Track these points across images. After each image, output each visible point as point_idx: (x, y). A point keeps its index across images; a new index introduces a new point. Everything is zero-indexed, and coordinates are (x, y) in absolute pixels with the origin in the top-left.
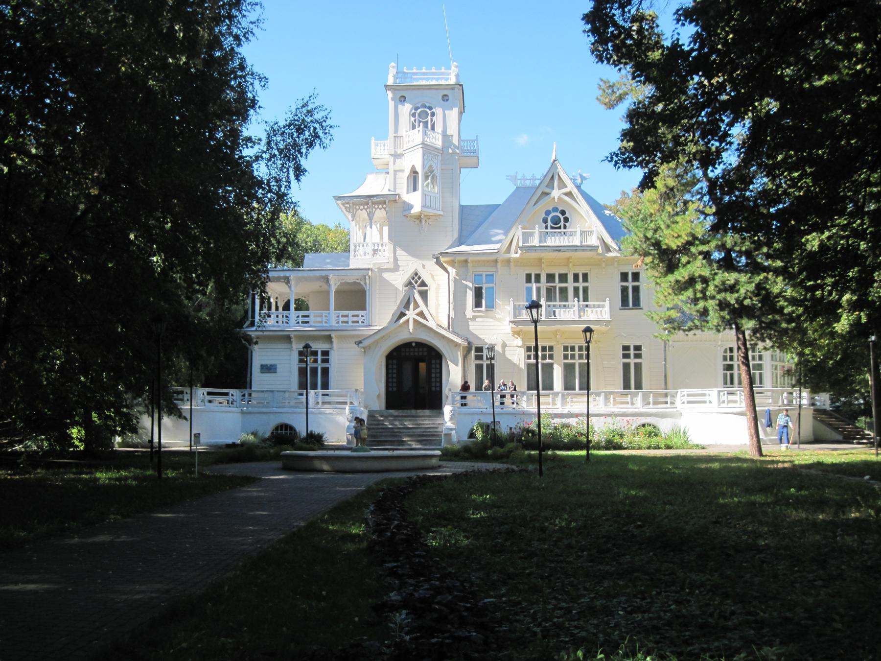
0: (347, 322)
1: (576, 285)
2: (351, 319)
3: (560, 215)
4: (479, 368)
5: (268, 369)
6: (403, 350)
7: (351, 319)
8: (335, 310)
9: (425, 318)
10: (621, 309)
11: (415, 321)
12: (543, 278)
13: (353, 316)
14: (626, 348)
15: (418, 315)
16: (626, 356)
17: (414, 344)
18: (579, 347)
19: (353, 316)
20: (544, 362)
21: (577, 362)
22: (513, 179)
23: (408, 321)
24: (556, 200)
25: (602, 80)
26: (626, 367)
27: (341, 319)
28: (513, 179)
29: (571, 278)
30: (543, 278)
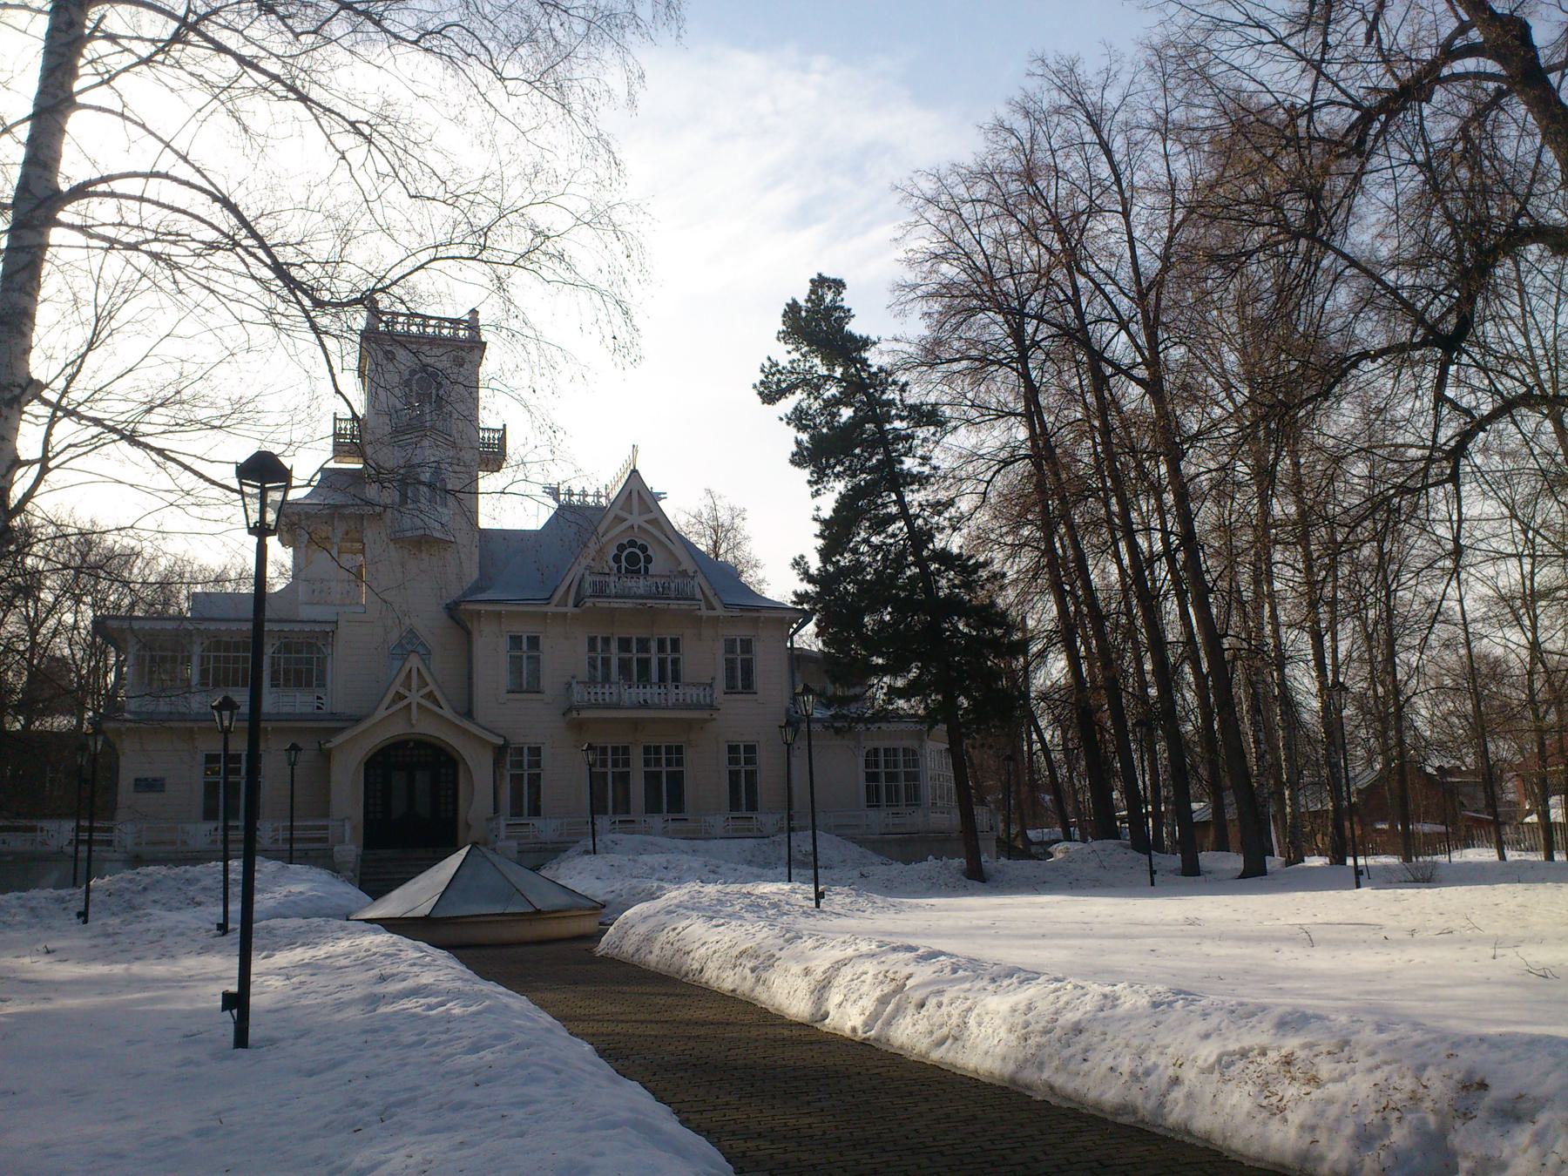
1: (662, 655)
4: (517, 779)
12: (614, 645)
14: (733, 749)
20: (670, 769)
26: (734, 775)
30: (614, 645)
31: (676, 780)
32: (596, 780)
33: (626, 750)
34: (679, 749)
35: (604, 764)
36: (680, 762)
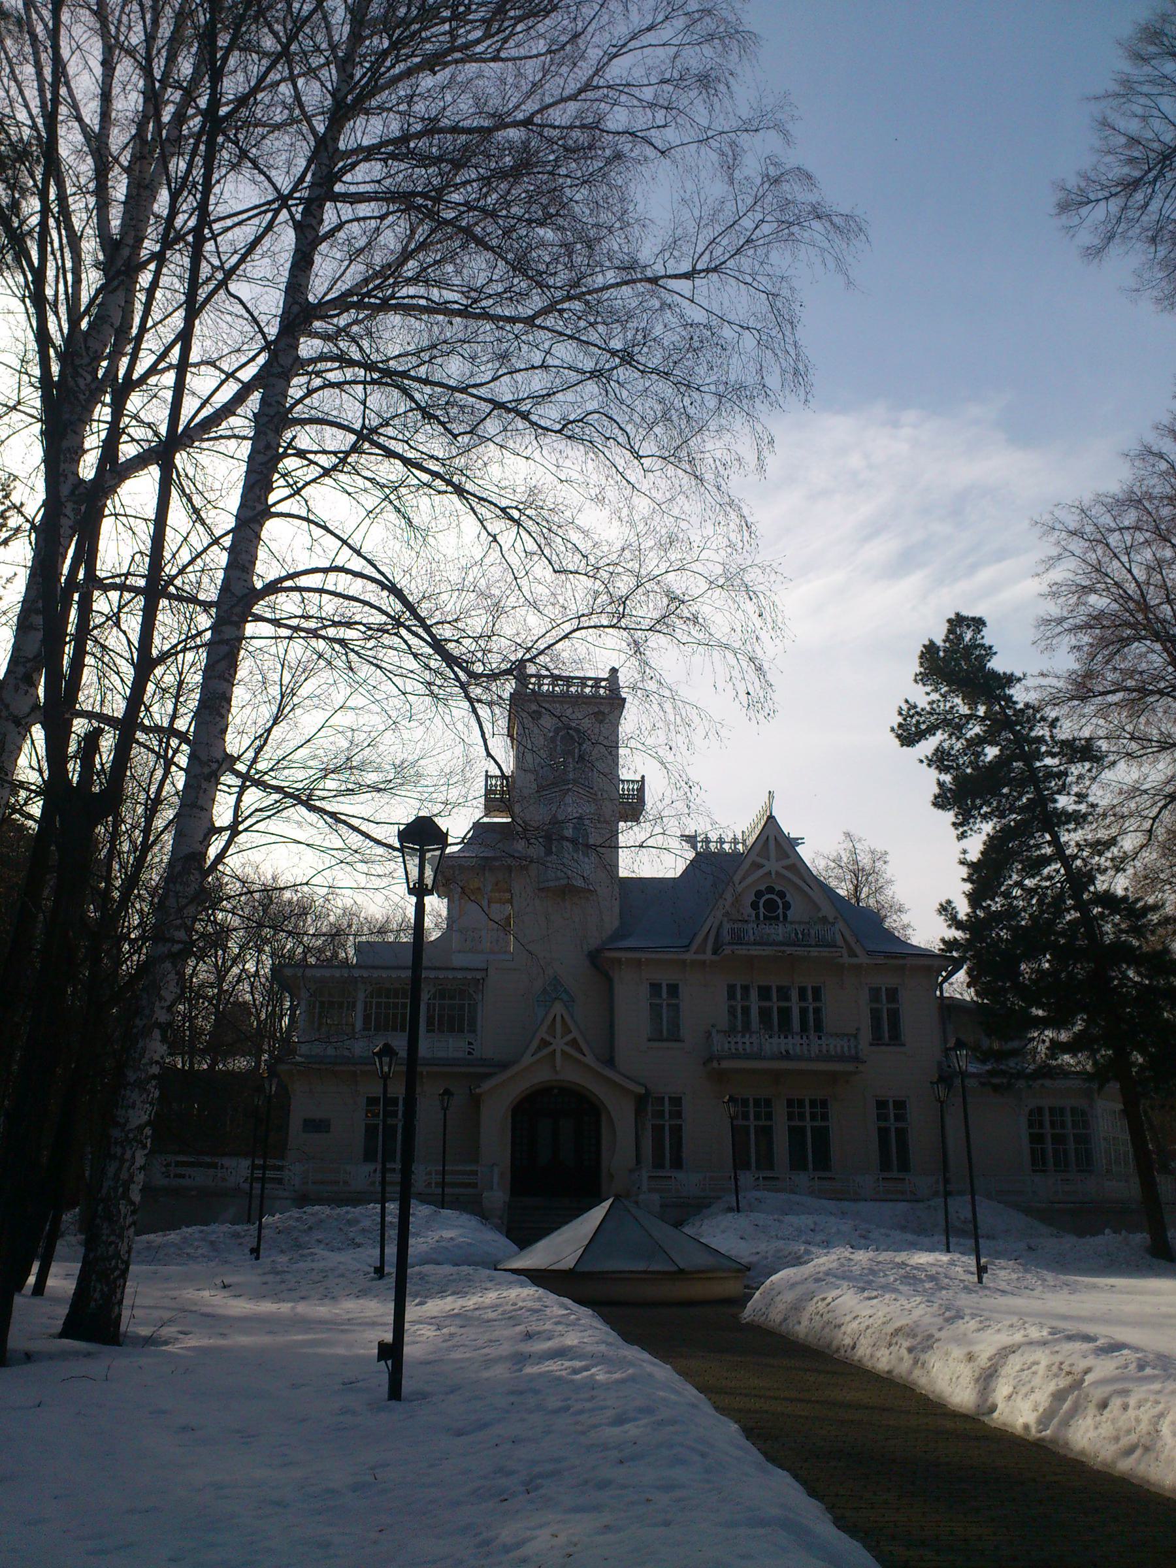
1: (804, 1004)
3: (764, 899)
4: (658, 1130)
5: (316, 1126)
9: (539, 1049)
10: (871, 1045)
11: (563, 1053)
14: (881, 1104)
16: (880, 1117)
17: (556, 1091)
18: (810, 1100)
21: (808, 1124)
25: (907, 701)
26: (883, 1133)
28: (691, 840)
29: (794, 995)
30: (754, 994)
31: (822, 1138)
32: (737, 1135)
33: (768, 1102)
34: (824, 1104)
35: (746, 1116)
36: (825, 1117)
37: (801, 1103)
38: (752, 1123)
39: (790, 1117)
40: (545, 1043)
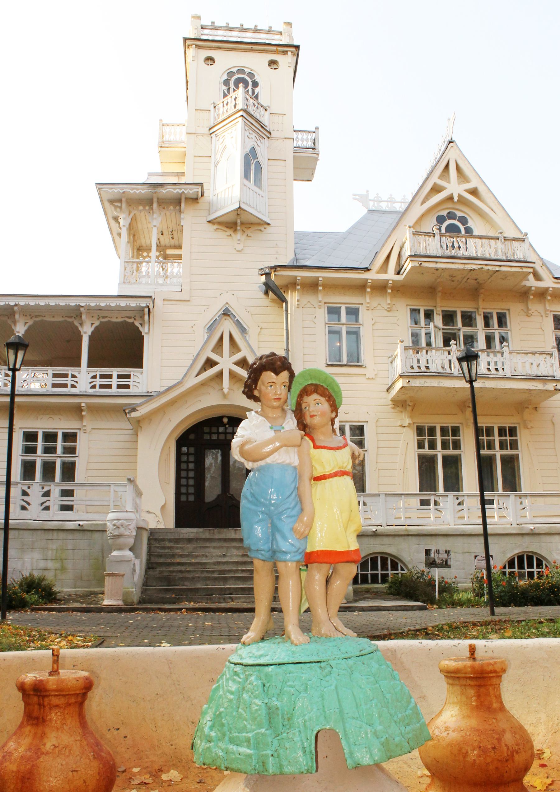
0: (109, 386)
2: (115, 381)
6: (206, 429)
7: (115, 381)
8: (90, 365)
13: (119, 377)
15: (237, 363)
17: (225, 420)
19: (119, 377)
21: (498, 453)
22: (362, 199)
23: (220, 375)
24: (456, 199)
27: (98, 381)
28: (362, 199)
29: (480, 321)
33: (456, 431)
34: (513, 431)
35: (432, 445)
36: (514, 445)
37: (490, 431)
38: (439, 452)
39: (479, 446)
40: (210, 363)
